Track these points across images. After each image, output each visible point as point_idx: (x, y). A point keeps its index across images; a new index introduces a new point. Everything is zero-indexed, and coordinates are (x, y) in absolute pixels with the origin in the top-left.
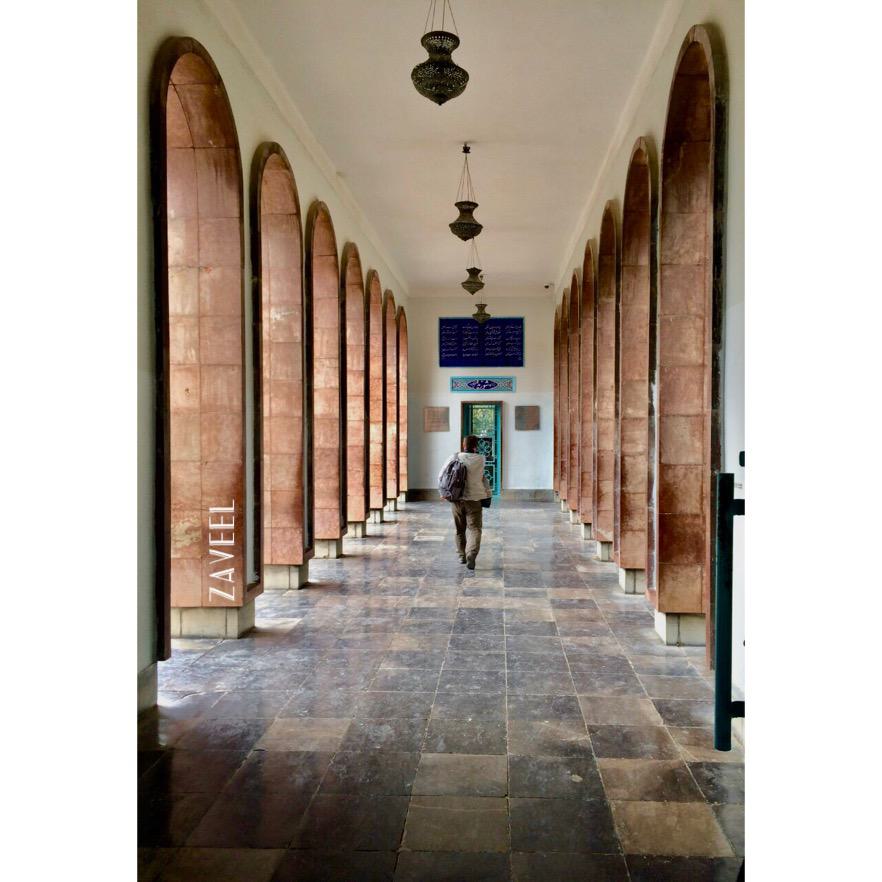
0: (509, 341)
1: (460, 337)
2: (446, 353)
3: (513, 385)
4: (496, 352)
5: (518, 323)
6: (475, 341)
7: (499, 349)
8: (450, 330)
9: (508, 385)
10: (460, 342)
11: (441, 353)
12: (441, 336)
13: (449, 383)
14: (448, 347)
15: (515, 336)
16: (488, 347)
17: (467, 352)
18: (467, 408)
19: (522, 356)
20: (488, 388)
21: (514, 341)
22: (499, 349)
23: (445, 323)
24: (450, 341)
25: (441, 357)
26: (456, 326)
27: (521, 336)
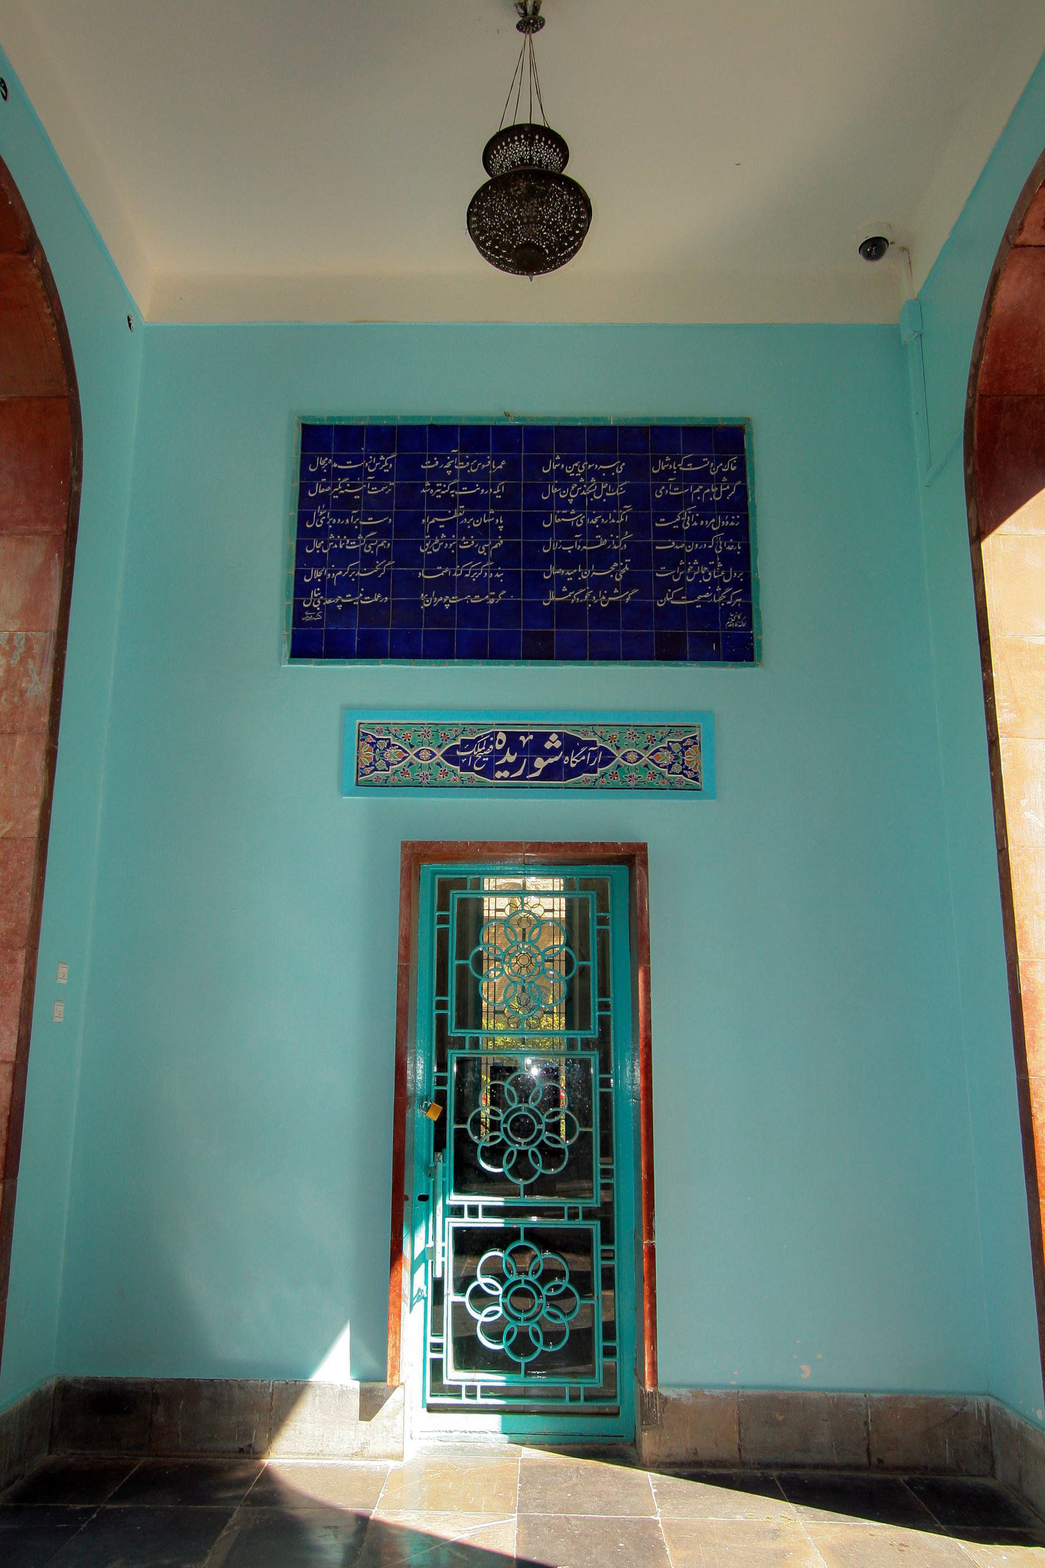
0: (674, 534)
1: (405, 519)
2: (327, 588)
3: (702, 760)
4: (598, 585)
5: (724, 444)
6: (485, 533)
7: (619, 570)
8: (353, 474)
9: (677, 761)
10: (408, 527)
11: (301, 590)
12: (306, 507)
13: (328, 754)
14: (343, 557)
15: (705, 508)
16: (565, 560)
17: (445, 586)
18: (438, 887)
19: (747, 610)
20: (549, 773)
21: (705, 534)
22: (619, 570)
23: (316, 438)
24: (350, 532)
25: (298, 612)
26: (386, 462)
27: (738, 506)
